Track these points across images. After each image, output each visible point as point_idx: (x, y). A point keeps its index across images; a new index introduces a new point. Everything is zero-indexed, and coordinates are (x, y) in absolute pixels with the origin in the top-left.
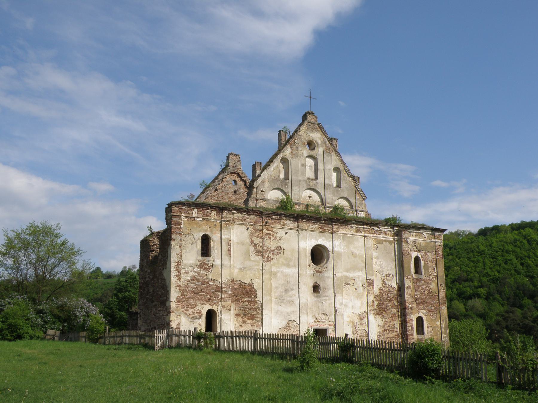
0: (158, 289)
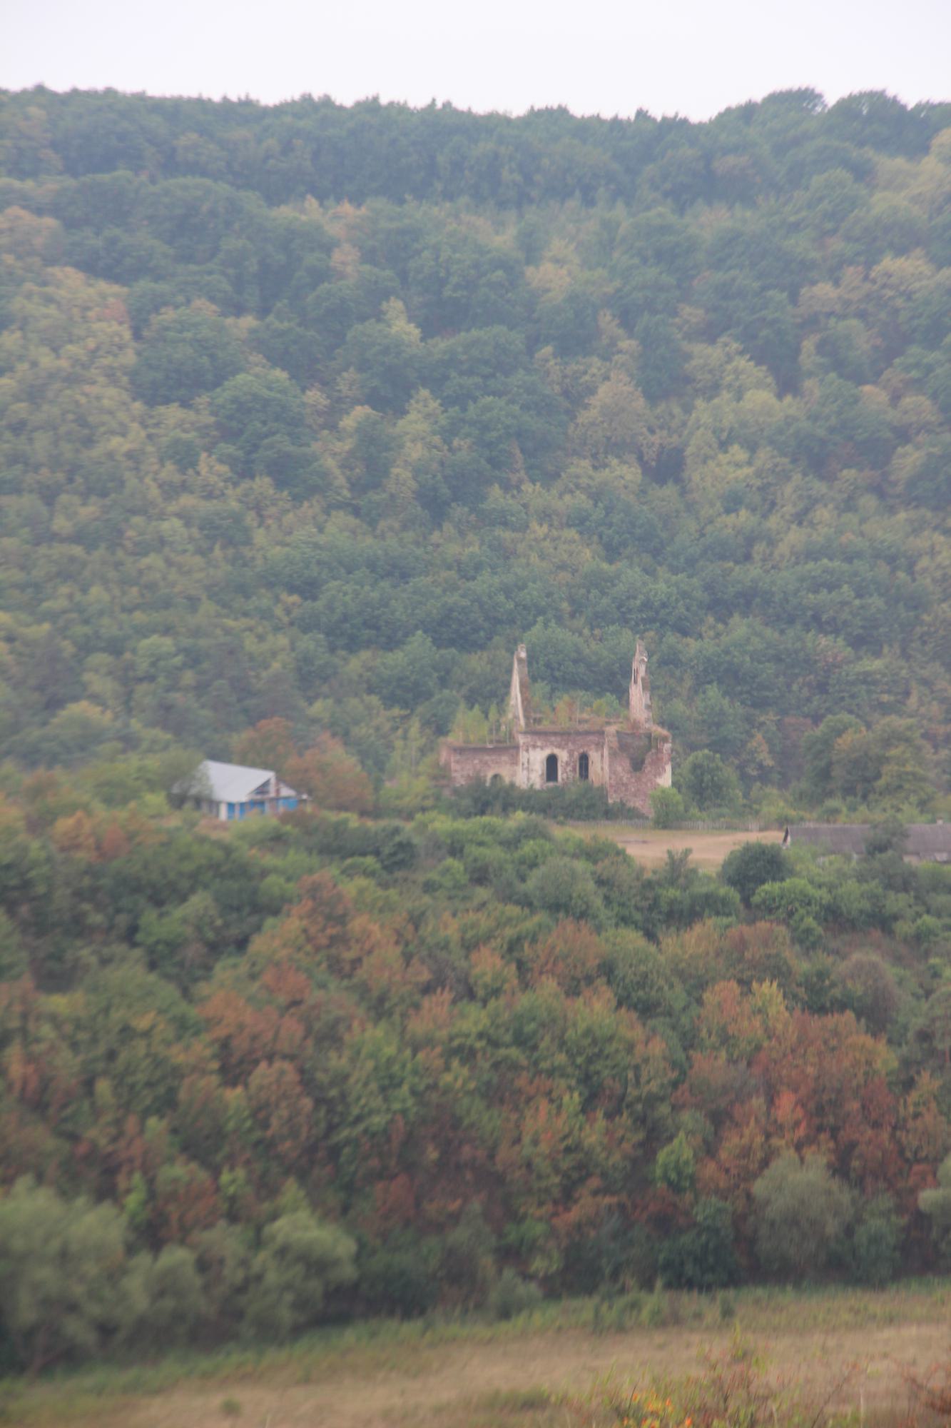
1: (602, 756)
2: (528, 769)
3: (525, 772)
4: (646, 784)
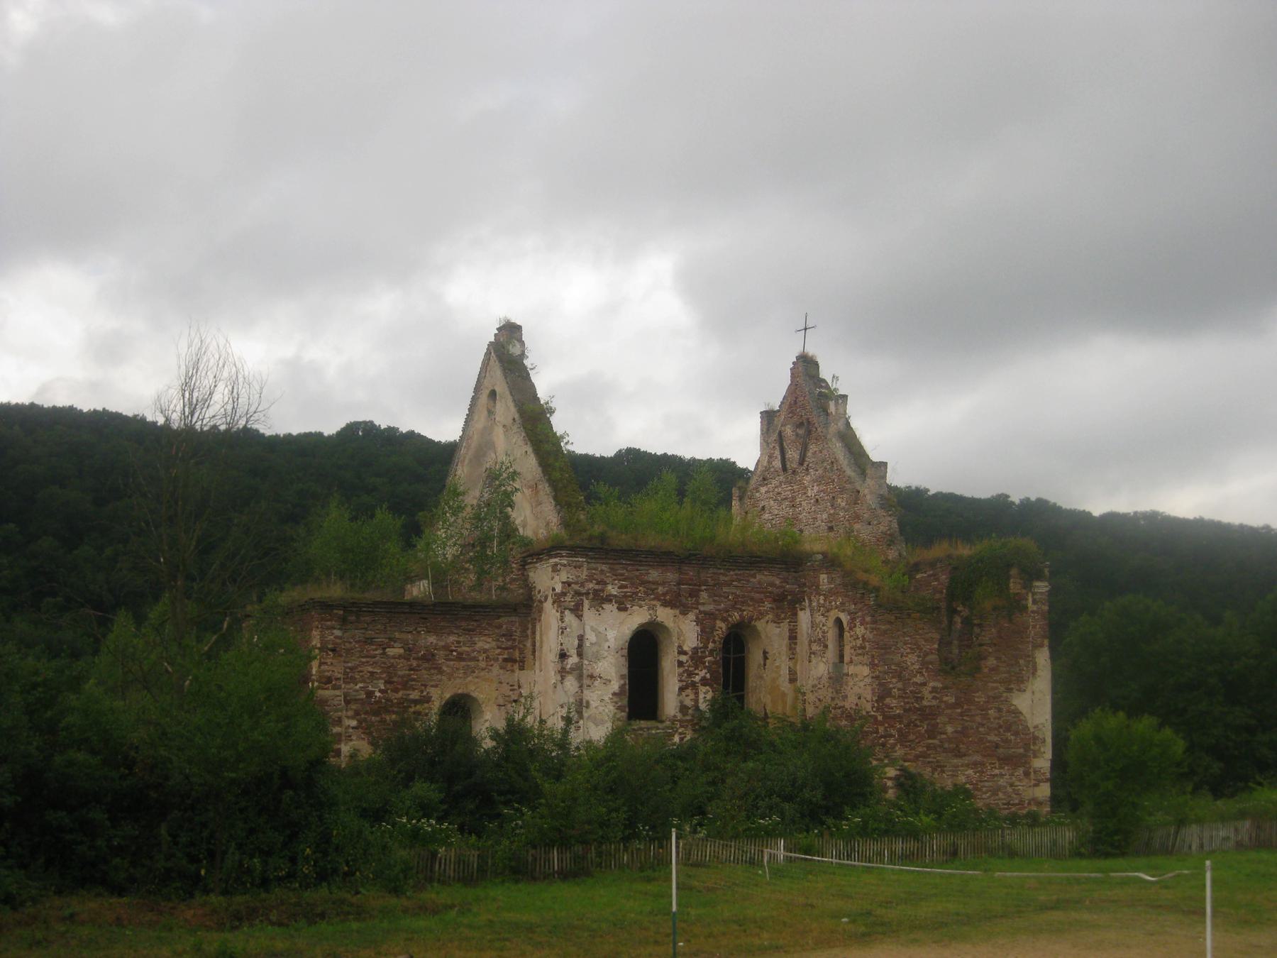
0: (981, 729)
1: (793, 637)
2: (578, 671)
3: (571, 683)
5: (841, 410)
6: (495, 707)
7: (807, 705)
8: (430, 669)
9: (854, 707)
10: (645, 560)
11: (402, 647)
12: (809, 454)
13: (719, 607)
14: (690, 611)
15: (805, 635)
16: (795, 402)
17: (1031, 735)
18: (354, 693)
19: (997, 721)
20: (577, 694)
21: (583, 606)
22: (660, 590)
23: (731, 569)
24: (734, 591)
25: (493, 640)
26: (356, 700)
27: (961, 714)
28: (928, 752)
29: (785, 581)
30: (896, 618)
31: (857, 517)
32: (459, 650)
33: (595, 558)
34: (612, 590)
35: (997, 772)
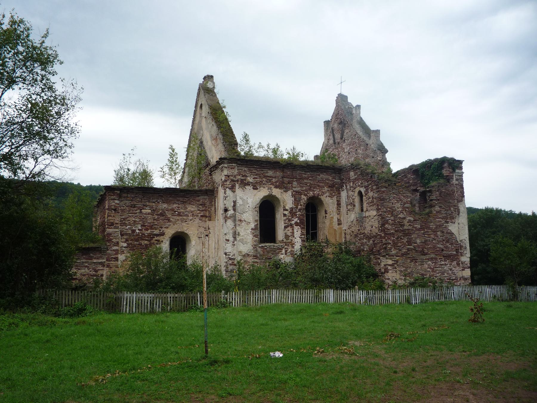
0: (434, 242)
1: (339, 204)
2: (234, 217)
3: (230, 223)
4: (435, 232)
5: (358, 112)
6: (197, 238)
7: (347, 235)
8: (164, 219)
9: (370, 232)
10: (265, 166)
11: (150, 209)
12: (345, 134)
13: (303, 189)
14: (289, 190)
15: (345, 202)
16: (338, 114)
17: (459, 245)
18: (126, 231)
19: (442, 238)
20: (233, 229)
21: (235, 187)
22: (274, 180)
23: (308, 172)
24: (310, 182)
25: (196, 207)
26: (126, 234)
27: (424, 234)
28: (408, 252)
29: (334, 178)
30: (389, 185)
31: (368, 156)
32: (179, 211)
33: (242, 165)
34: (250, 179)
35: (443, 263)
